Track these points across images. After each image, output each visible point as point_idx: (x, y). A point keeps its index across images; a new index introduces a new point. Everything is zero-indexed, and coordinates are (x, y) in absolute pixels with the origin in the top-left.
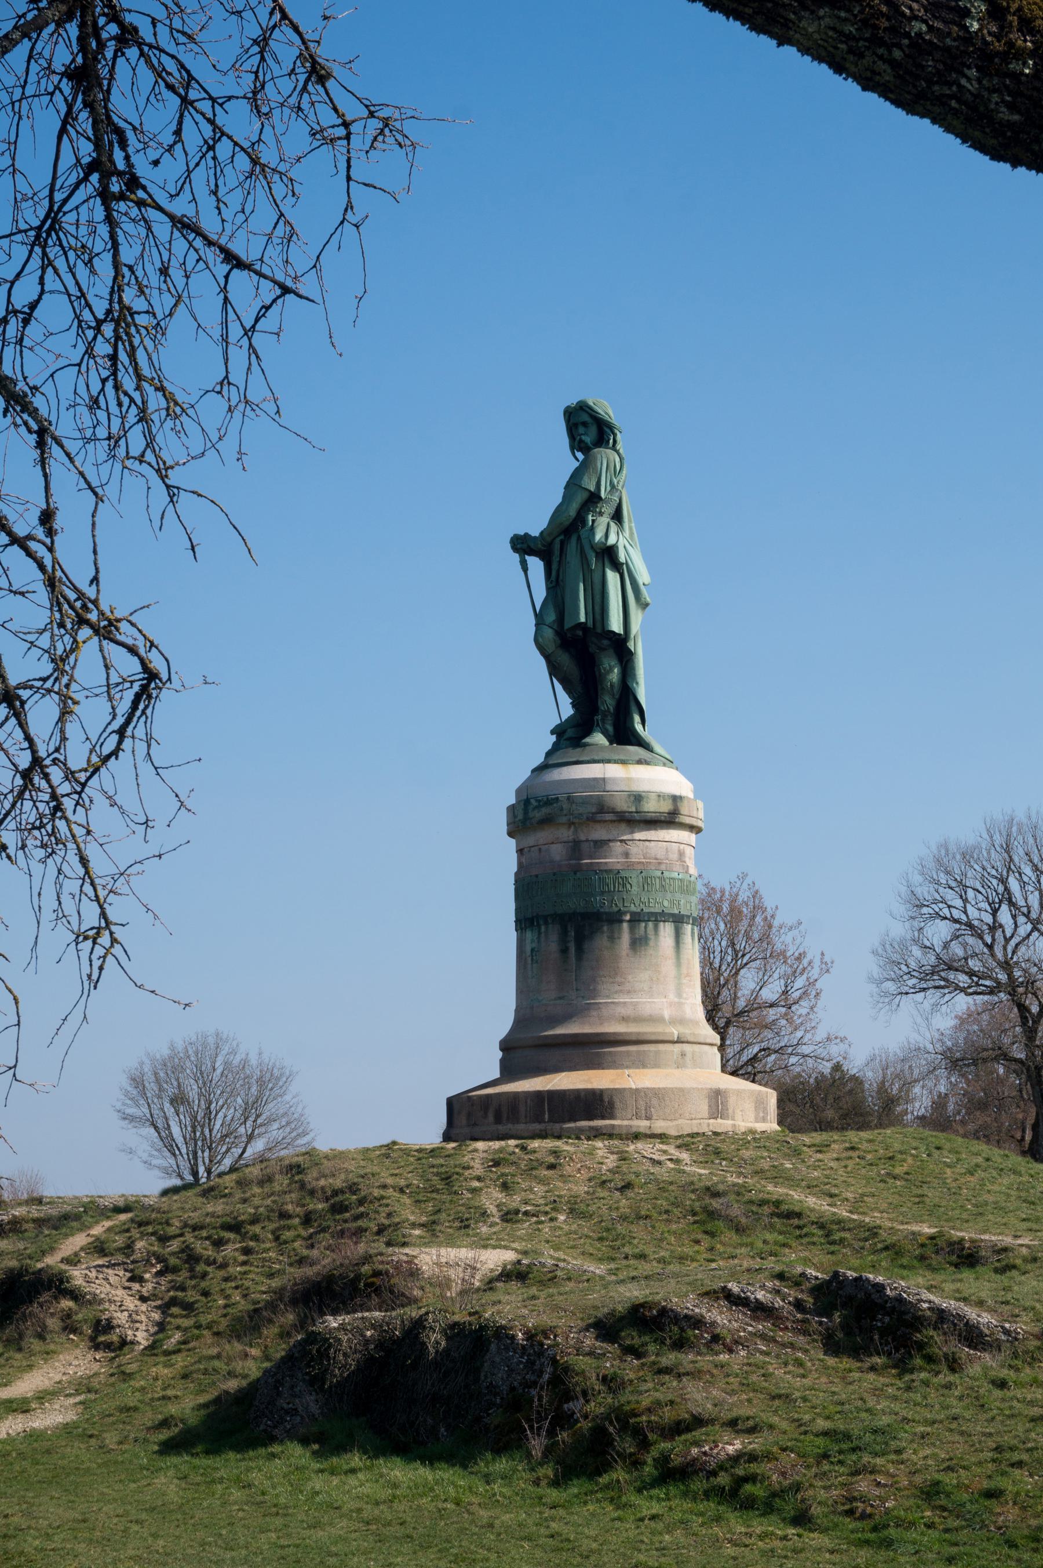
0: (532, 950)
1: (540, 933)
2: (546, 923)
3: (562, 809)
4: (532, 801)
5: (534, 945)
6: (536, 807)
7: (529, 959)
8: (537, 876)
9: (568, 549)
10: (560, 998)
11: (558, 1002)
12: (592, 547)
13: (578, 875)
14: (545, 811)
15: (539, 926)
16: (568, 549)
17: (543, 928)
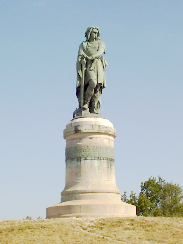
0: (98, 166)
1: (101, 161)
2: (103, 159)
3: (109, 130)
4: (102, 126)
5: (99, 165)
6: (102, 128)
7: (97, 169)
8: (100, 146)
9: (85, 63)
10: (108, 180)
11: (107, 181)
12: (105, 65)
13: (110, 148)
14: (106, 129)
15: (101, 159)
16: (85, 63)
17: (102, 160)
